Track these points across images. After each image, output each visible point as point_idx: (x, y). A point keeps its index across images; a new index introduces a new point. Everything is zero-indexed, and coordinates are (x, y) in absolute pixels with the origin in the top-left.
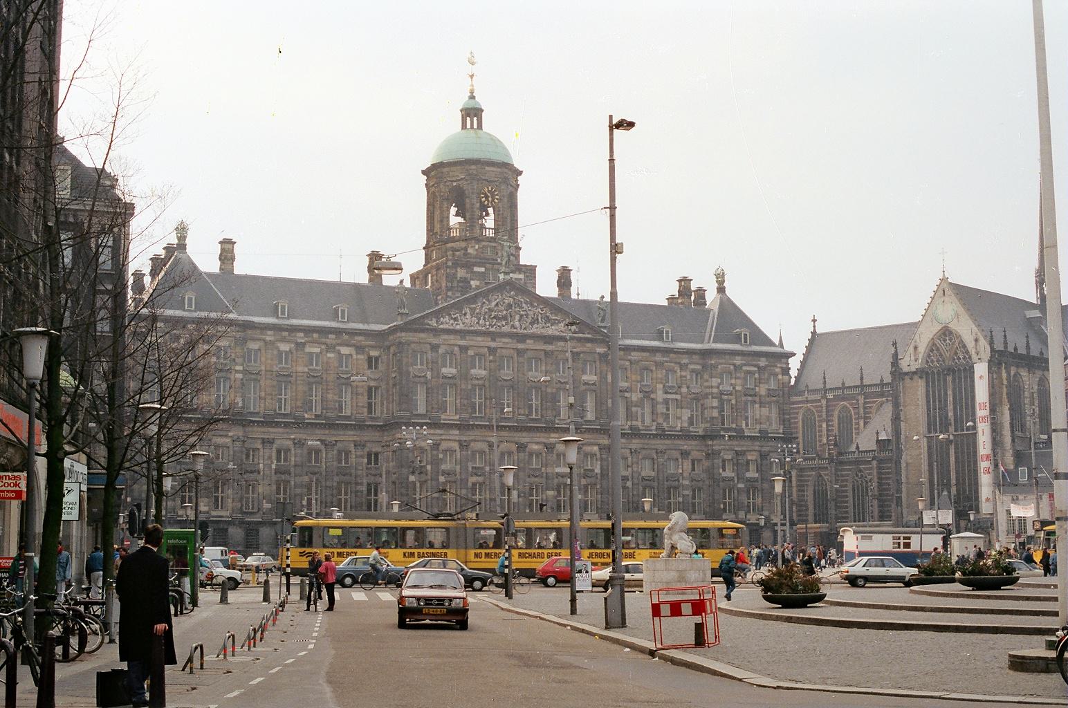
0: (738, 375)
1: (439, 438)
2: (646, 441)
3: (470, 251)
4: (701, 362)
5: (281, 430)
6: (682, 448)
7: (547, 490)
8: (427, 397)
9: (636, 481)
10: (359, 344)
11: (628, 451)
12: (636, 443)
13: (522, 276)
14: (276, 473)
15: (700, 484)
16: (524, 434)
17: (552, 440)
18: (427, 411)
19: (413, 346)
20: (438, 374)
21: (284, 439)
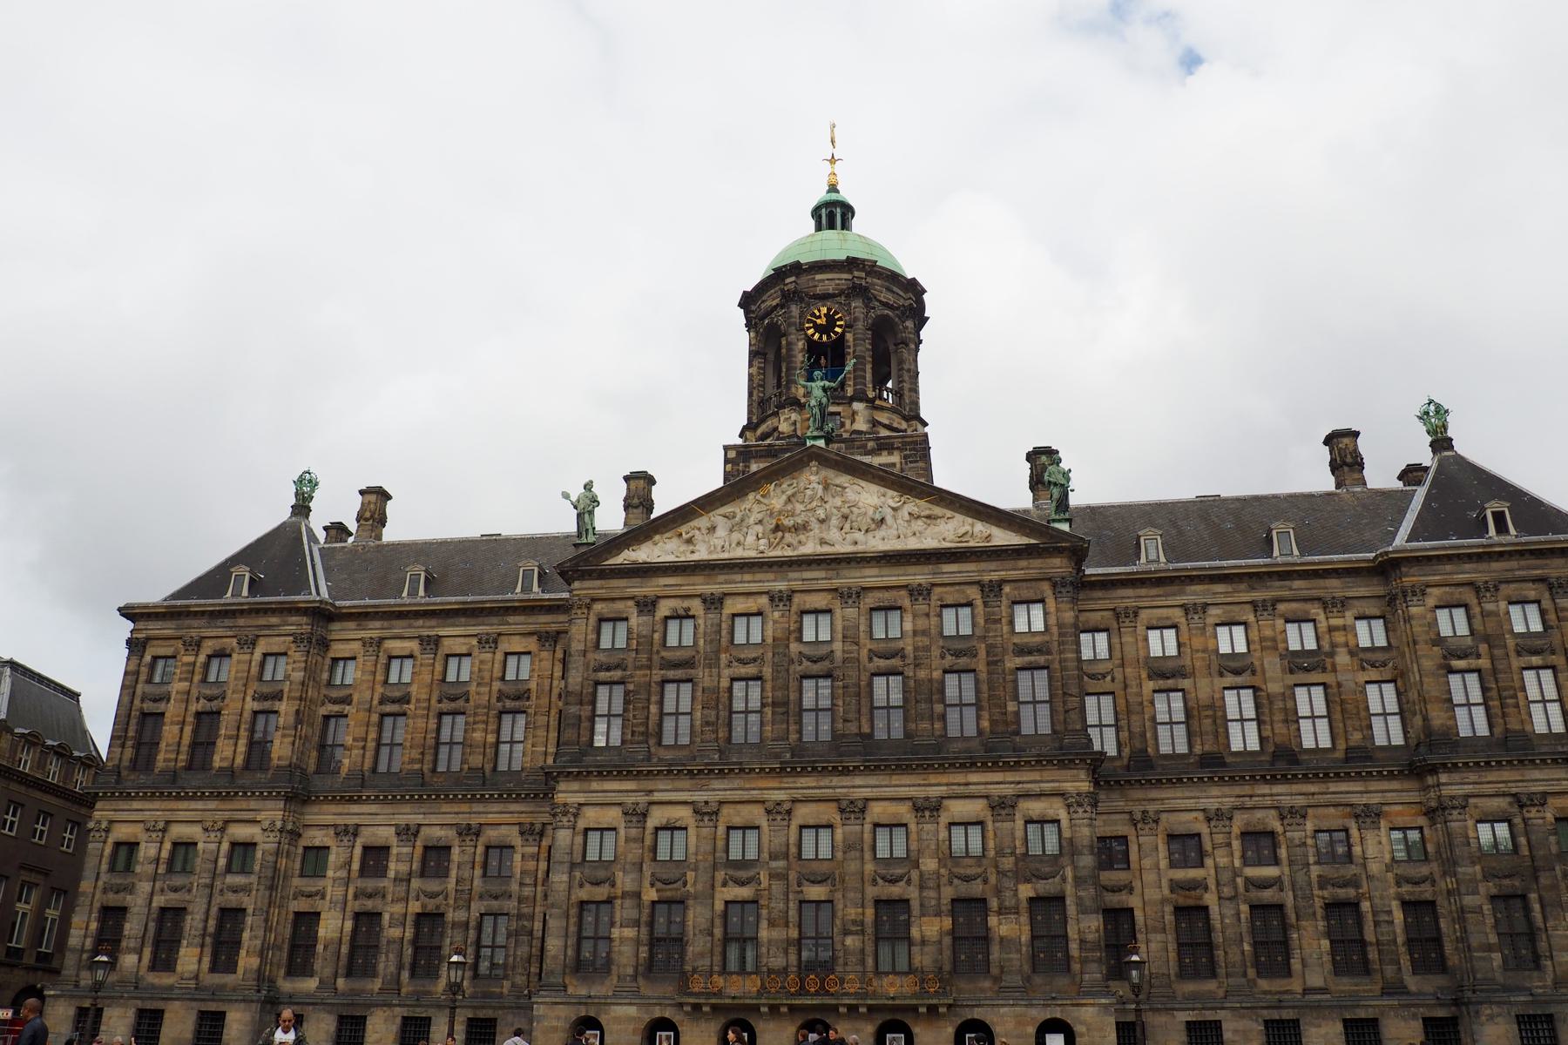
0: (1490, 607)
1: (642, 799)
2: (1247, 790)
3: (784, 427)
4: (1380, 590)
5: (373, 808)
6: (1355, 799)
7: (923, 915)
8: (625, 710)
9: (1227, 891)
10: (543, 628)
11: (1200, 816)
12: (1216, 797)
13: (895, 458)
14: (356, 897)
15: (1425, 892)
16: (858, 781)
17: (935, 792)
18: (623, 742)
19: (598, 607)
20: (650, 659)
21: (380, 823)
